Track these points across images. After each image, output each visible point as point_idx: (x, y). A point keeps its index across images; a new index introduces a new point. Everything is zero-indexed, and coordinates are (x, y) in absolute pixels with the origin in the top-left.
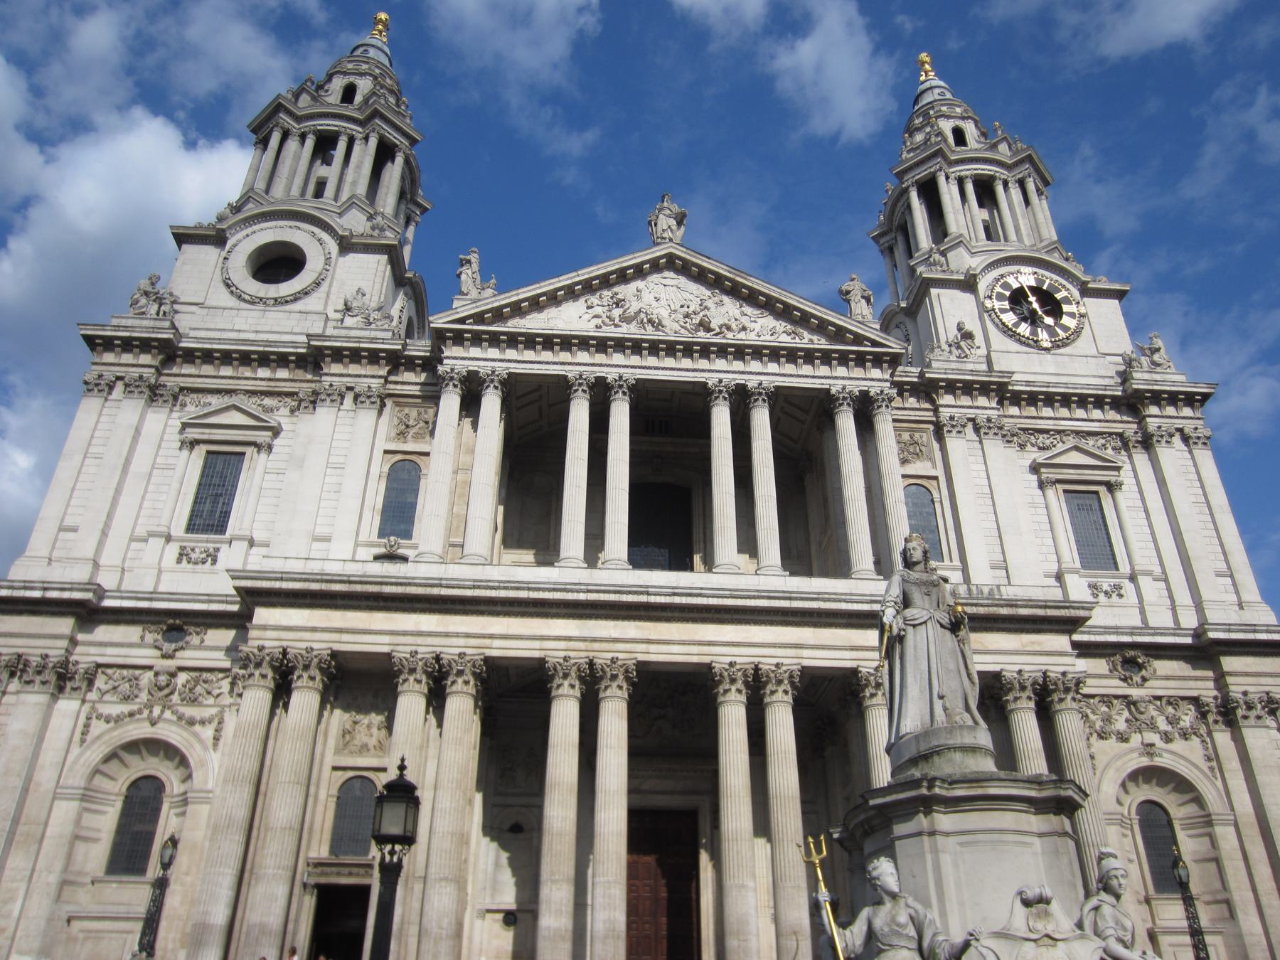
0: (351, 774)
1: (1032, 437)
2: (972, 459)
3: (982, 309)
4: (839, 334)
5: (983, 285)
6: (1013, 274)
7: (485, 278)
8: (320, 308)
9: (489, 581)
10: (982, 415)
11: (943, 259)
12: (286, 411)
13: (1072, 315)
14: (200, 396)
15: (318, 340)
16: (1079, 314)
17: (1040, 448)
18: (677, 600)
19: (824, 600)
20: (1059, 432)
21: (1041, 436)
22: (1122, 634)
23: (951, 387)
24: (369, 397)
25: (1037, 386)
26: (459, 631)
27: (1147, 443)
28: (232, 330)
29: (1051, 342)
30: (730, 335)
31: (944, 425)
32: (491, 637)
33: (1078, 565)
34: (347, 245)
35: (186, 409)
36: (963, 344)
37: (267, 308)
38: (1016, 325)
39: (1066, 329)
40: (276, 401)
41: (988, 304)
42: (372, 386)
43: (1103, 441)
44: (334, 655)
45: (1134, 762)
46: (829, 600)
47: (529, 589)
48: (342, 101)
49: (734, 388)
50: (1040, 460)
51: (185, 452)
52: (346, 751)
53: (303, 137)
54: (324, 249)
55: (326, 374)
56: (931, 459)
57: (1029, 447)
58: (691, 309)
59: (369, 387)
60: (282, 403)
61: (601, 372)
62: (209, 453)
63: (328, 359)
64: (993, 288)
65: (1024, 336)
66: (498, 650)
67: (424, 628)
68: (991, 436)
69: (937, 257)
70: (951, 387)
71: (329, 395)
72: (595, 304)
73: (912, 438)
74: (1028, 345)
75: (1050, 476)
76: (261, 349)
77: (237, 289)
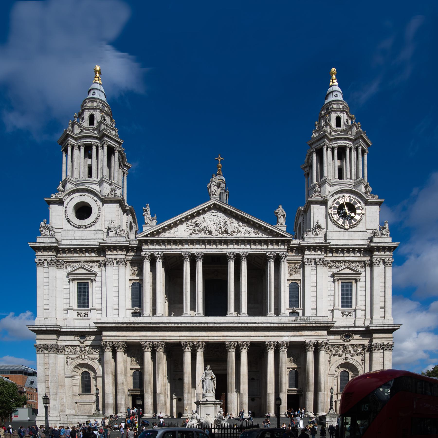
0: (135, 370)
1: (335, 264)
2: (312, 273)
3: (328, 214)
4: (271, 233)
5: (329, 203)
6: (341, 197)
7: (152, 216)
8: (99, 228)
9: (163, 322)
10: (318, 258)
11: (319, 189)
12: (97, 267)
13: (359, 214)
14: (70, 264)
15: (102, 243)
16: (362, 214)
17: (338, 268)
18: (216, 325)
19: (257, 324)
20: (344, 261)
21: (338, 263)
22: (346, 328)
23: (309, 248)
24: (121, 262)
25: (339, 246)
26: (157, 335)
27: (371, 265)
28: (74, 239)
29: (349, 226)
30: (235, 234)
31: (305, 262)
32: (166, 336)
33: (340, 307)
34: (104, 201)
35: (67, 268)
36: (317, 230)
37: (84, 230)
38: (338, 220)
39: (355, 220)
40: (93, 264)
41: (330, 211)
42: (122, 258)
43: (358, 264)
44: (125, 342)
45: (342, 362)
46: (258, 324)
47: (175, 324)
48: (90, 125)
49: (235, 255)
50: (335, 273)
51: (71, 283)
52: (133, 365)
53: (79, 147)
54: (97, 204)
55: (107, 255)
56: (300, 273)
57: (333, 267)
58: (222, 225)
59: (121, 259)
60: (95, 265)
61: (192, 251)
62: (77, 282)
63: (107, 250)
64: (333, 204)
65: (340, 224)
66: (168, 340)
67: (148, 335)
68: (320, 265)
69: (317, 188)
70: (309, 248)
71: (109, 262)
72: (190, 225)
73: (295, 266)
74: (341, 228)
75: (337, 277)
76: (85, 247)
77: (72, 222)
